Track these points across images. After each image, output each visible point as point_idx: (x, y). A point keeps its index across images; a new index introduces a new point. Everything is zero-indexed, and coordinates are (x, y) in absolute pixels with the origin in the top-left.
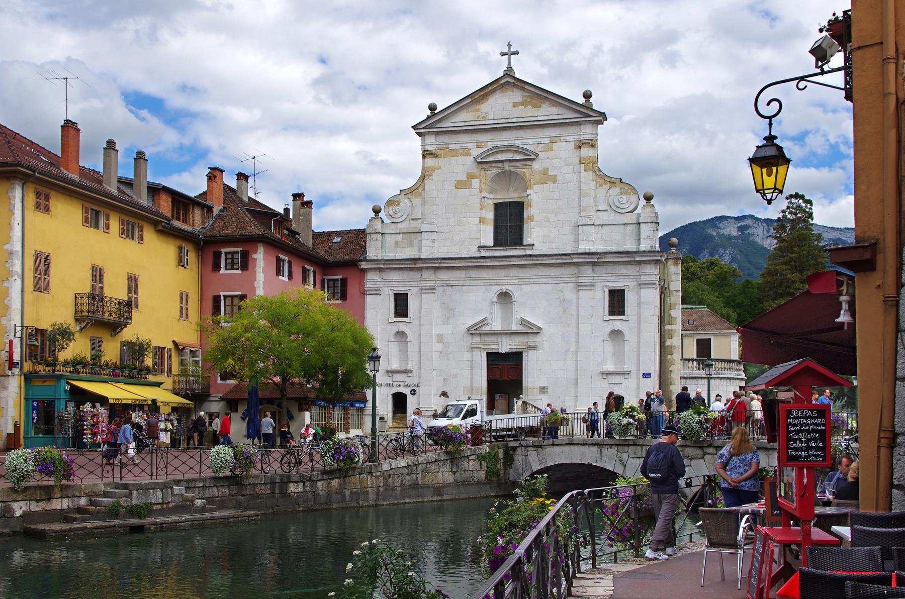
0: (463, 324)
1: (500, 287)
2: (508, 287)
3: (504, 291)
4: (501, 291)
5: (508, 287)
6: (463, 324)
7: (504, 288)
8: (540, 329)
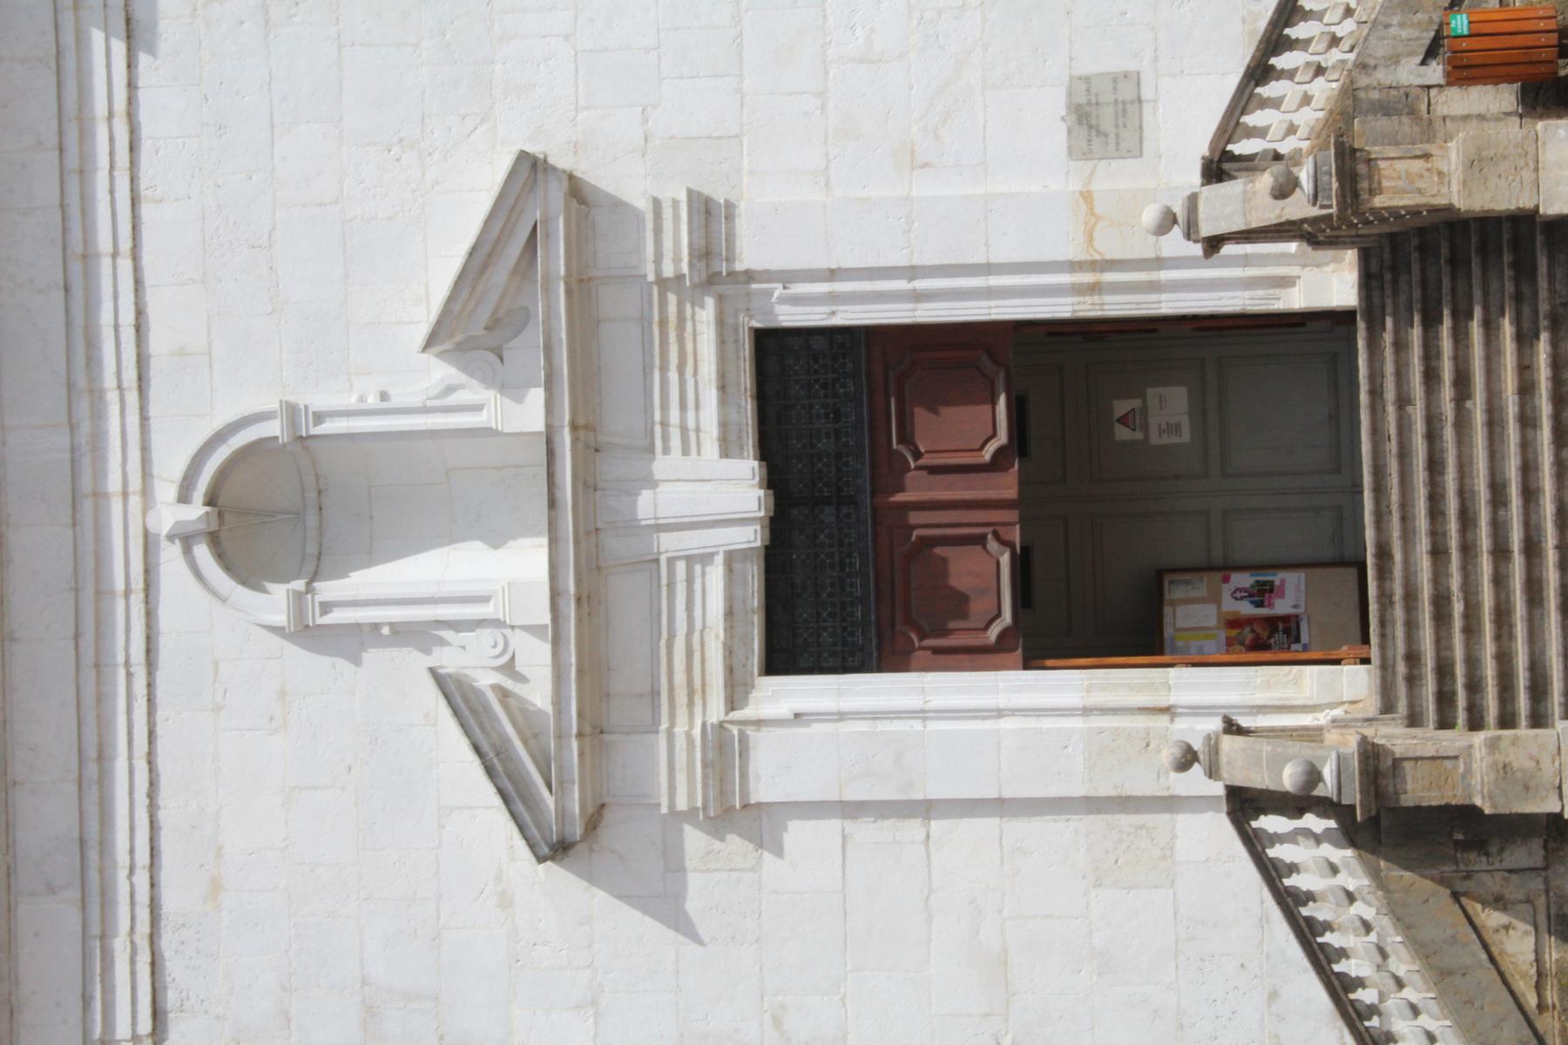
0: (505, 901)
1: (171, 558)
2: (166, 492)
3: (196, 511)
4: (202, 552)
5: (166, 492)
6: (505, 901)
7: (170, 514)
8: (530, 169)
